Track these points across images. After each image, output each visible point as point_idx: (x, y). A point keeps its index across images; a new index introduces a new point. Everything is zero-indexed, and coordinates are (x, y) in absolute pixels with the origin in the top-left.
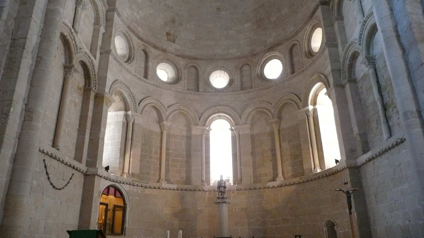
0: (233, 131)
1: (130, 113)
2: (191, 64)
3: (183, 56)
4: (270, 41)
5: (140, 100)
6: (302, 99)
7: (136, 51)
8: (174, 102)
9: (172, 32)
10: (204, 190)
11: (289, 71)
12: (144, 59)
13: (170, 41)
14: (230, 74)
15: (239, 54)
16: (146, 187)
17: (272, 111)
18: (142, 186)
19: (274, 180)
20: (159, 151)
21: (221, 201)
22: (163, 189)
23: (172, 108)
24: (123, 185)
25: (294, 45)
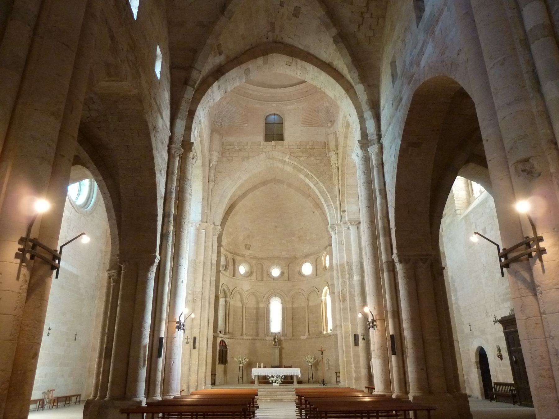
1: (227, 299)
2: (260, 262)
5: (232, 290)
7: (229, 260)
8: (249, 288)
10: (265, 340)
11: (315, 273)
13: (247, 249)
14: (282, 268)
15: (287, 256)
16: (236, 339)
17: (305, 295)
18: (234, 339)
19: (304, 335)
20: (241, 317)
22: (244, 339)
23: (249, 292)
24: (226, 339)
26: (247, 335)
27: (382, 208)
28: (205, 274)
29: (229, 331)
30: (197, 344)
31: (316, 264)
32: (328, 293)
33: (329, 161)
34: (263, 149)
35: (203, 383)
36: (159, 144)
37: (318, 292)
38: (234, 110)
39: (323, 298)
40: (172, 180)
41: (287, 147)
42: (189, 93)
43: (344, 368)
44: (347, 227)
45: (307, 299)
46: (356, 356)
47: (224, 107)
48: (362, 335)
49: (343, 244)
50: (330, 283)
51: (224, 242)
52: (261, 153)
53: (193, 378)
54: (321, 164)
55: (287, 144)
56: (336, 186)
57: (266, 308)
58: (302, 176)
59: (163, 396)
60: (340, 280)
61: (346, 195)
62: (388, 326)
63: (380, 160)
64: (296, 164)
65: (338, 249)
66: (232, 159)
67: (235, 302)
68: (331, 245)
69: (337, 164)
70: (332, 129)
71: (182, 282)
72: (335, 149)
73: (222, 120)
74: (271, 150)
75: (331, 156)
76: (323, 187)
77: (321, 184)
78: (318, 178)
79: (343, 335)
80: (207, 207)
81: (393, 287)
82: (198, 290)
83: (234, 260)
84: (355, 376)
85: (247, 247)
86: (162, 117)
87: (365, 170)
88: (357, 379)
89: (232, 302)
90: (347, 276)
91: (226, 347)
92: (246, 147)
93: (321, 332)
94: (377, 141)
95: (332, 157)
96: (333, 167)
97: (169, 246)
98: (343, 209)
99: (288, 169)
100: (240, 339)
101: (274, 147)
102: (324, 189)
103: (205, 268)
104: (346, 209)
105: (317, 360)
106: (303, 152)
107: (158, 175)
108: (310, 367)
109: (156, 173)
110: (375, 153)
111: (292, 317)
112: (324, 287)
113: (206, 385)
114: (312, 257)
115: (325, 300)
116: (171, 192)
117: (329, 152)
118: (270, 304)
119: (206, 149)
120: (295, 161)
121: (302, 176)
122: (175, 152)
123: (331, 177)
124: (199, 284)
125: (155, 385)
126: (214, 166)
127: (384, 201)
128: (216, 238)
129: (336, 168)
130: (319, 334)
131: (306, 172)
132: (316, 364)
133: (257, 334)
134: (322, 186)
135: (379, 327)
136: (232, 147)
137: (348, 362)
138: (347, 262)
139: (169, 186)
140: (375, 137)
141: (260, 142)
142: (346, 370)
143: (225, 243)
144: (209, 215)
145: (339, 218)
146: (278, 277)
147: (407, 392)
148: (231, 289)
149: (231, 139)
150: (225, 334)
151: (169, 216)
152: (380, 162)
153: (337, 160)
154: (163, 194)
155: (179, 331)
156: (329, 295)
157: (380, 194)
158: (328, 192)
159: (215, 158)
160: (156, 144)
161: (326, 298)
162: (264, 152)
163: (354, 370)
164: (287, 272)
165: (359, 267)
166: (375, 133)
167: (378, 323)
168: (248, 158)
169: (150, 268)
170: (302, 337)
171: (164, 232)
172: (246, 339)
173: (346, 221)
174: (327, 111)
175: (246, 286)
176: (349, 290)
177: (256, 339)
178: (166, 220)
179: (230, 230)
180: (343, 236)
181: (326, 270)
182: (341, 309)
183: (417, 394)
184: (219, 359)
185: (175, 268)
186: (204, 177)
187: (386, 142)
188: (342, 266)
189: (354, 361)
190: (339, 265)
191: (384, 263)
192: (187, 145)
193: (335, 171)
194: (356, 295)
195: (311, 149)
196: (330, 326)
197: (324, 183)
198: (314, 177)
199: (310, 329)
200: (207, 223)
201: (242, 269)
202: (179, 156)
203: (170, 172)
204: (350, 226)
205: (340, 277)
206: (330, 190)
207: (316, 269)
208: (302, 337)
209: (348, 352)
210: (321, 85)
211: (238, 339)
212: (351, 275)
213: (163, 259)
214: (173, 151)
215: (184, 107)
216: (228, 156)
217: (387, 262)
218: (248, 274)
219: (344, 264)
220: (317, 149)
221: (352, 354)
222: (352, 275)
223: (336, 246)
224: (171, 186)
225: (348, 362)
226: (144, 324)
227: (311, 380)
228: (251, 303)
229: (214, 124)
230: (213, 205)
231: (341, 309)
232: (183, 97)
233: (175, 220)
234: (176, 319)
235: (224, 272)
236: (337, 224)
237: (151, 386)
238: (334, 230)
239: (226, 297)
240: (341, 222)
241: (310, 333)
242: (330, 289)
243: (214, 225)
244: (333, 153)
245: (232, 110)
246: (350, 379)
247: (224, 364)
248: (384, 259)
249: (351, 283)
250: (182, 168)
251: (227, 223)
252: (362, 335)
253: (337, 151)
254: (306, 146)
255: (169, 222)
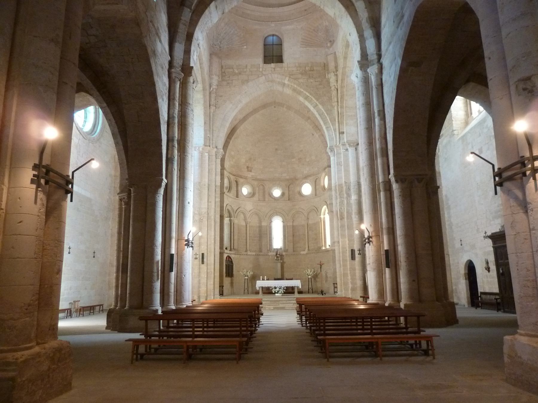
0: (284, 223)
1: (232, 218)
2: (260, 184)
3: (256, 180)
4: (305, 172)
6: (319, 211)
8: (252, 208)
9: (250, 166)
10: (268, 255)
11: (314, 193)
12: (236, 185)
14: (283, 189)
15: (288, 177)
17: (305, 214)
18: (239, 254)
19: (304, 251)
21: (277, 261)
23: (251, 212)
25: (317, 179)
26: (251, 251)
27: (380, 131)
28: (210, 196)
29: (235, 248)
30: (205, 260)
31: (316, 184)
32: (327, 211)
33: (328, 82)
34: (262, 71)
35: (212, 294)
36: (159, 68)
37: (317, 211)
38: (232, 31)
39: (322, 216)
40: (174, 104)
41: (286, 69)
42: (186, 15)
43: (341, 279)
44: (346, 149)
45: (306, 217)
46: (353, 269)
47: (222, 29)
48: (358, 250)
49: (341, 165)
50: (328, 203)
51: (227, 165)
52: (260, 76)
53: (203, 289)
54: (320, 86)
55: (286, 66)
56: (336, 108)
57: (268, 227)
58: (301, 99)
59: (176, 305)
60: (338, 200)
61: (345, 117)
62: (383, 242)
63: (379, 80)
64: (295, 86)
65: (336, 170)
66: (232, 83)
67: (239, 221)
68: (329, 166)
69: (336, 86)
70: (331, 49)
71: (189, 203)
72: (335, 70)
73: (220, 42)
74: (271, 72)
75: (331, 78)
76: (322, 109)
77: (320, 107)
78: (317, 100)
79: (341, 250)
80: (210, 131)
81: (389, 205)
82: (204, 211)
83: (236, 182)
84: (352, 287)
85: (249, 169)
86: (160, 41)
87: (365, 91)
88: (353, 289)
89: (236, 221)
90: (345, 195)
91: (232, 262)
92: (245, 70)
93: (320, 248)
94: (376, 61)
95: (332, 78)
96: (332, 89)
97: (174, 169)
98: (341, 131)
99: (288, 91)
100: (245, 255)
101: (273, 70)
102: (324, 111)
103: (210, 190)
104: (345, 131)
105: (317, 273)
106: (302, 74)
107: (160, 100)
108: (310, 280)
109: (158, 98)
110: (374, 74)
111: (293, 234)
112: (323, 206)
113: (215, 296)
114: (311, 178)
115: (324, 218)
116: (174, 117)
117: (328, 73)
118: (272, 223)
119: (206, 74)
120: (295, 84)
121: (301, 99)
122: (175, 77)
123: (330, 99)
124: (205, 205)
125: (169, 295)
126: (215, 90)
127: (382, 122)
128: (219, 161)
129: (336, 89)
130: (318, 250)
131: (306, 94)
132: (315, 277)
133: (260, 251)
134: (321, 108)
135: (374, 243)
136: (231, 70)
137: (345, 275)
138: (346, 183)
139: (171, 111)
140: (375, 57)
141: (259, 65)
142: (343, 281)
143: (228, 166)
144: (211, 139)
145: (338, 140)
146: (279, 197)
147: (398, 301)
148: (235, 209)
149: (230, 62)
150: (230, 250)
151: (173, 140)
152: (380, 83)
153: (336, 82)
154: (166, 119)
155: (188, 248)
156: (328, 213)
157: (379, 115)
158: (327, 114)
159: (215, 82)
160: (156, 69)
161: (325, 216)
162: (263, 74)
163: (351, 282)
164: (288, 192)
165: (356, 187)
166: (375, 52)
167: (374, 239)
168: (247, 81)
169: (158, 191)
170: (302, 253)
171: (169, 156)
172: (250, 255)
173: (345, 142)
174: (327, 31)
175: (249, 206)
176: (347, 209)
177: (260, 255)
178: (170, 144)
179: (233, 153)
180: (341, 157)
181: (325, 190)
182: (339, 227)
183: (408, 303)
184: (226, 273)
185: (181, 190)
186: (205, 102)
187: (386, 61)
188: (340, 186)
189: (350, 273)
190: (337, 186)
191: (381, 183)
192: (187, 70)
193: (334, 93)
194: (353, 214)
195: (310, 70)
196: (328, 242)
197: (322, 104)
198: (314, 99)
199: (309, 245)
200: (210, 146)
201: (245, 191)
202: (180, 80)
203: (172, 97)
204: (348, 148)
205: (338, 197)
206: (329, 112)
207: (316, 190)
208: (302, 253)
209: (345, 266)
210: (321, 2)
211: (243, 255)
212: (349, 195)
213: (169, 181)
214: (174, 75)
215: (182, 29)
216: (228, 80)
217: (384, 182)
218: (250, 195)
219: (342, 184)
220: (317, 70)
221: (349, 267)
222: (350, 195)
223: (335, 167)
224: (173, 111)
225: (345, 275)
226: (155, 242)
227: (311, 290)
228: (254, 221)
229: (213, 47)
230: (214, 129)
231: (339, 227)
232: (181, 19)
233: (179, 144)
234: (184, 237)
235: (228, 194)
236: (336, 146)
237: (166, 297)
238: (333, 151)
239: (230, 216)
240: (340, 144)
241: (310, 249)
242: (329, 208)
243: (217, 149)
244: (332, 74)
245: (231, 32)
246: (346, 289)
247: (230, 277)
248: (381, 179)
249: (348, 202)
250: (183, 93)
251: (229, 147)
252: (358, 250)
253: (337, 72)
254: (305, 67)
255: (173, 146)
